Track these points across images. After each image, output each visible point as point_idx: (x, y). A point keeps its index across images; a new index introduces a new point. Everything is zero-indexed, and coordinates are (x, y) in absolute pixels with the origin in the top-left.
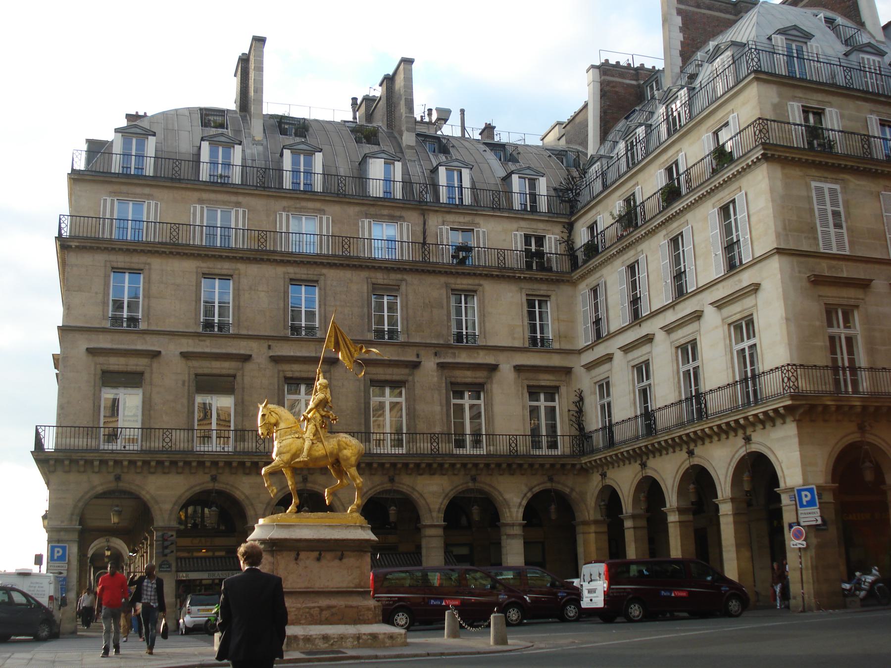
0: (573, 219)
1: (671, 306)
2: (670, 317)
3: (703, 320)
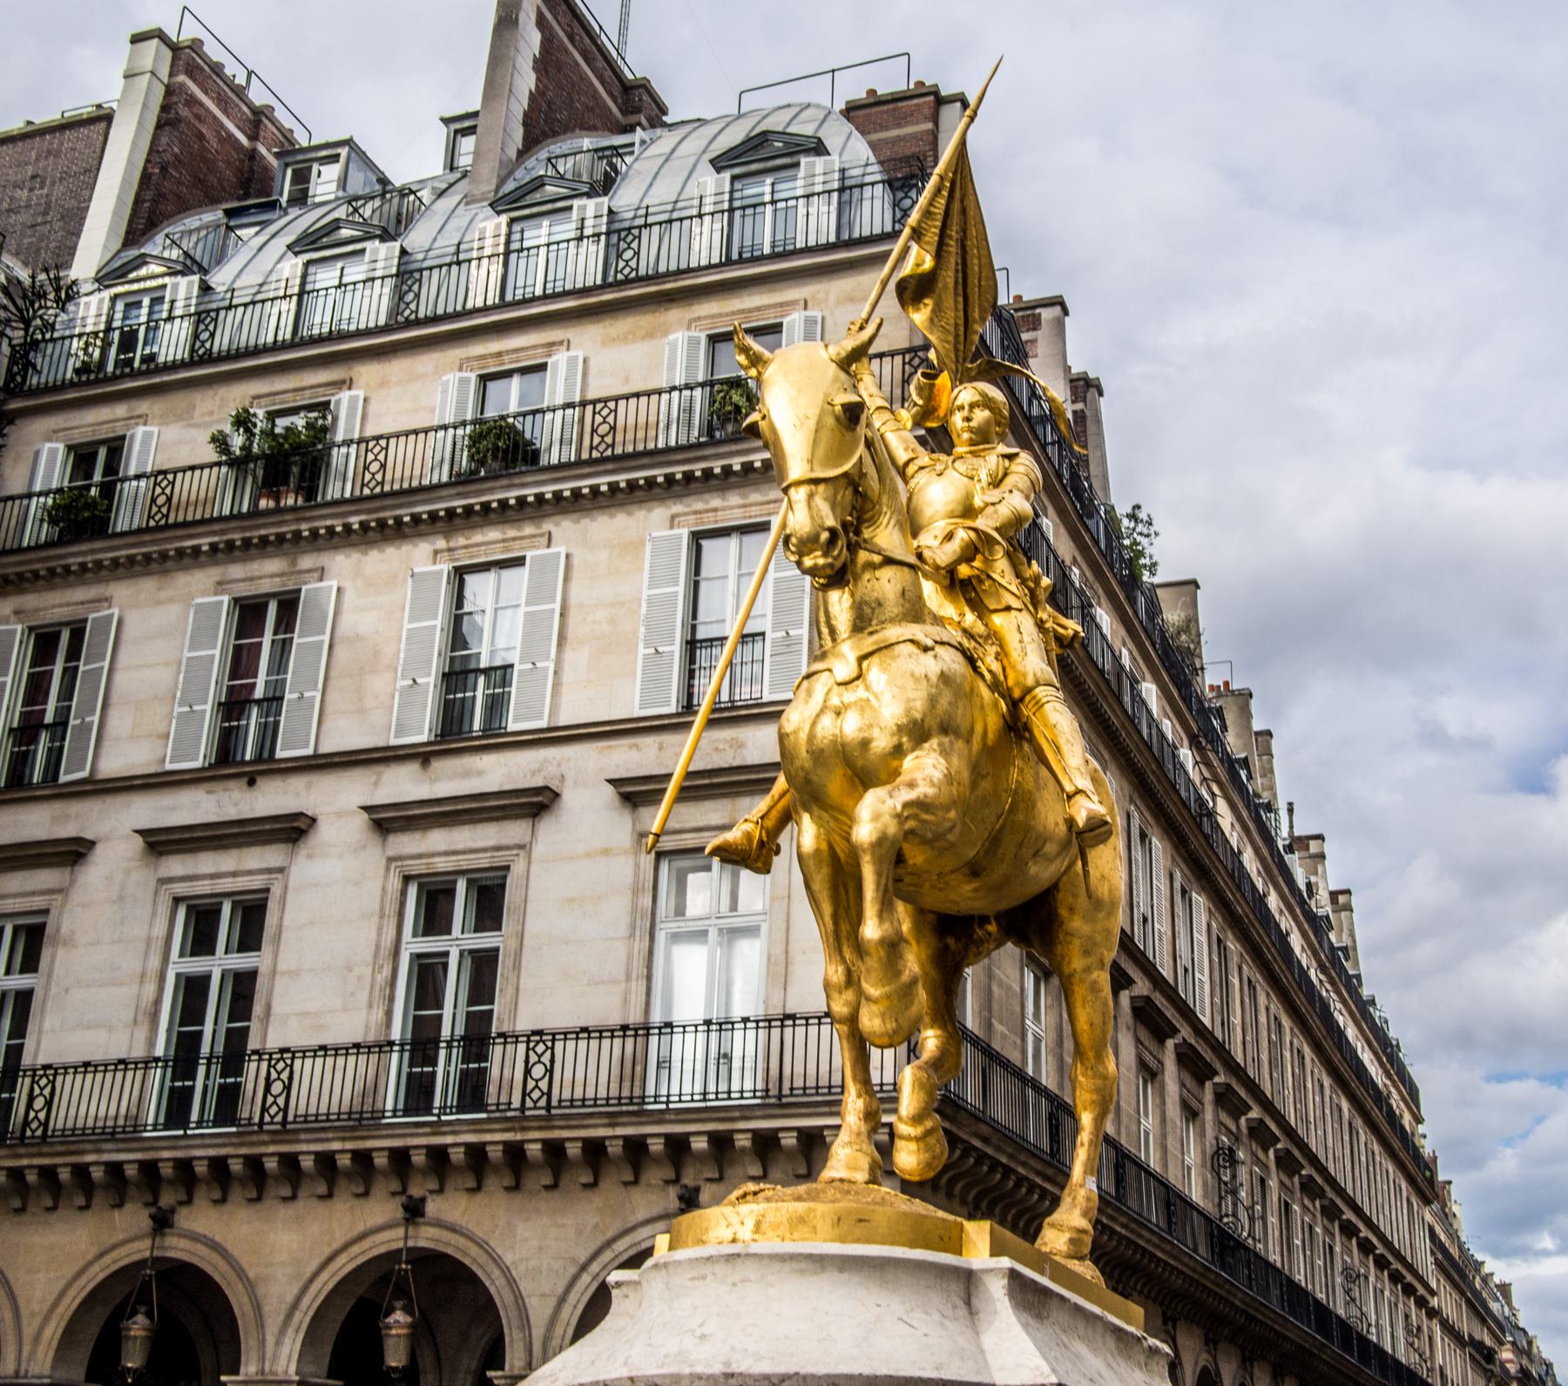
0: (15, 405)
1: (422, 756)
2: (403, 785)
3: (546, 825)
